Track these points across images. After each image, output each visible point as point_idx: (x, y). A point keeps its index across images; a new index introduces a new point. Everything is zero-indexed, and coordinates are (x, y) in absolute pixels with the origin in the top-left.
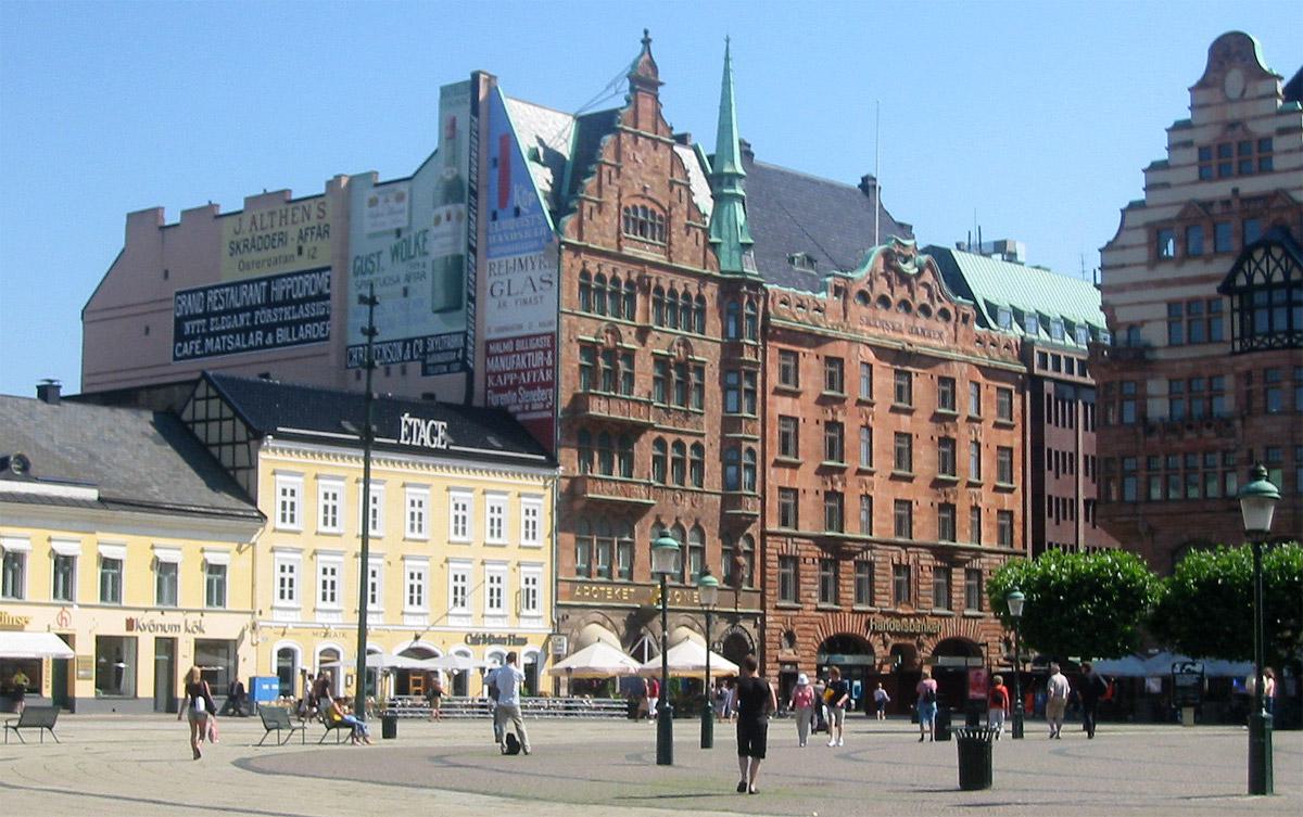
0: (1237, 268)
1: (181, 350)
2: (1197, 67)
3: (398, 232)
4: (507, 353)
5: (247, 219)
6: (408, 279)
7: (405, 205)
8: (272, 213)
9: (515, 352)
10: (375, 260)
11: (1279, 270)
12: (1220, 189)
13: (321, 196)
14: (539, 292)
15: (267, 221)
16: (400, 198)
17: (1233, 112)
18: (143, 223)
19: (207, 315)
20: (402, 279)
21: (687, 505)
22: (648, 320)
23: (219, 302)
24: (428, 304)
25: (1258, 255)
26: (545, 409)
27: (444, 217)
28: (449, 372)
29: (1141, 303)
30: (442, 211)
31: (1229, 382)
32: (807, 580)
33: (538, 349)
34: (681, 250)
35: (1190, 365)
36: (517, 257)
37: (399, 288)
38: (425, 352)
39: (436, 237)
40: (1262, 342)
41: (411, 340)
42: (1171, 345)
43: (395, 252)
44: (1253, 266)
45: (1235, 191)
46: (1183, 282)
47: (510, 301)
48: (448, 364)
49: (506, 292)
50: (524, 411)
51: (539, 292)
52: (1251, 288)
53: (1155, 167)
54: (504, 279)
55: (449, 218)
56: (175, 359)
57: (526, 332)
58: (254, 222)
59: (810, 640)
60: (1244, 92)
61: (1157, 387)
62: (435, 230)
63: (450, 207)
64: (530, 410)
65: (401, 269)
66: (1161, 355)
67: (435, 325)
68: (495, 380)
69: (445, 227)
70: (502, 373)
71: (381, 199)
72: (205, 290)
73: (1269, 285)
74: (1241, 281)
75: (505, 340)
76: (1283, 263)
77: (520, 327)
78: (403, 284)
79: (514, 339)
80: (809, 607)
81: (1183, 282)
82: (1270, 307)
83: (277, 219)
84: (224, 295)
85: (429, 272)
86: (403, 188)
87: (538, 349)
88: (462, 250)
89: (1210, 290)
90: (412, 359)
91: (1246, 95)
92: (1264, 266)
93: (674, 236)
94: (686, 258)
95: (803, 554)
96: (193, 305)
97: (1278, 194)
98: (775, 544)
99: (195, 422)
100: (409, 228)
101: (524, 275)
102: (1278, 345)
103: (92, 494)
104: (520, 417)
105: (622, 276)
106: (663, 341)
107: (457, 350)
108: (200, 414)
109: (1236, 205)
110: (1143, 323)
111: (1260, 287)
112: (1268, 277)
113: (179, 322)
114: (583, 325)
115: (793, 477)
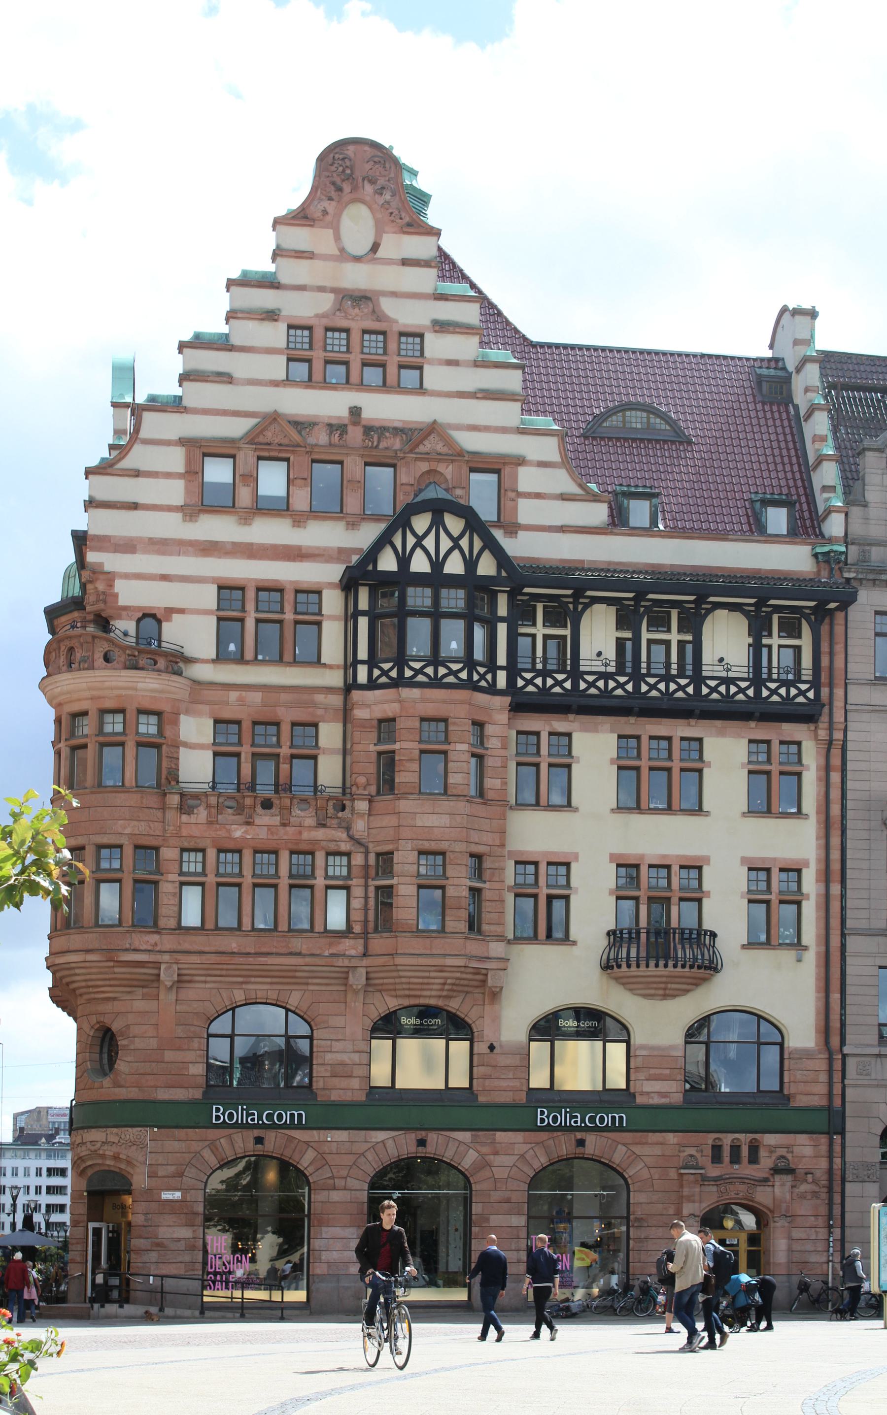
0: (384, 540)
2: (296, 186)
11: (456, 554)
12: (330, 404)
17: (356, 277)
25: (421, 523)
29: (165, 578)
31: (330, 734)
35: (256, 697)
40: (420, 671)
42: (221, 657)
44: (411, 541)
45: (355, 412)
46: (251, 551)
52: (405, 576)
53: (198, 343)
60: (375, 247)
61: (195, 729)
66: (204, 672)
73: (436, 579)
74: (388, 562)
76: (464, 543)
81: (251, 551)
82: (436, 615)
89: (334, 572)
91: (381, 253)
92: (429, 543)
97: (433, 429)
102: (451, 679)
109: (355, 435)
110: (170, 611)
111: (420, 580)
112: (437, 564)
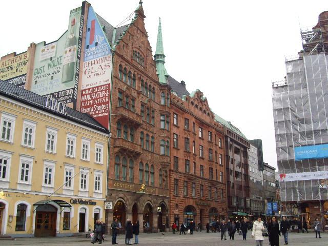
4: (90, 94)
9: (93, 92)
10: (42, 69)
20: (51, 73)
26: (105, 112)
33: (103, 90)
36: (96, 59)
37: (50, 76)
38: (58, 97)
41: (53, 94)
43: (49, 65)
48: (66, 100)
49: (91, 72)
50: (96, 114)
54: (90, 68)
55: (70, 51)
64: (99, 114)
65: (51, 70)
68: (84, 104)
69: (69, 53)
71: (46, 49)
75: (90, 89)
79: (93, 88)
85: (61, 70)
87: (103, 90)
104: (95, 116)
105: (132, 72)
107: (70, 95)
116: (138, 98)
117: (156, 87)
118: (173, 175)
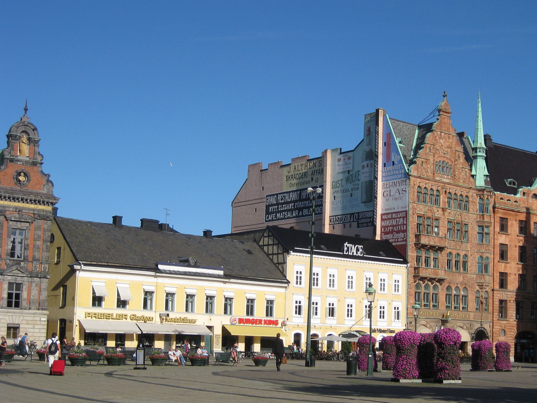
1: (268, 218)
3: (349, 171)
5: (292, 167)
6: (352, 190)
7: (351, 161)
8: (301, 165)
9: (392, 218)
13: (320, 158)
14: (401, 195)
15: (300, 168)
16: (349, 158)
18: (258, 171)
19: (278, 204)
20: (350, 190)
21: (461, 279)
22: (445, 205)
23: (282, 199)
24: (360, 199)
27: (366, 166)
28: (367, 226)
30: (365, 163)
32: (511, 309)
34: (459, 178)
36: (393, 181)
37: (349, 193)
38: (358, 218)
39: (363, 173)
41: (353, 214)
47: (391, 198)
48: (367, 223)
49: (389, 195)
50: (395, 242)
51: (401, 195)
54: (388, 190)
55: (367, 166)
56: (266, 221)
57: (396, 210)
58: (295, 168)
59: (512, 333)
62: (362, 171)
63: (368, 162)
64: (398, 241)
67: (362, 208)
68: (384, 230)
69: (366, 169)
70: (387, 227)
72: (277, 195)
75: (389, 214)
77: (394, 209)
78: (351, 192)
79: (392, 213)
80: (511, 320)
83: (303, 167)
84: (284, 197)
85: (360, 187)
86: (350, 154)
87: (401, 217)
88: (373, 179)
90: (354, 221)
93: (456, 173)
94: (461, 181)
95: (510, 299)
96: (273, 200)
98: (497, 295)
99: (264, 245)
100: (353, 170)
101: (396, 188)
103: (221, 273)
104: (394, 244)
105: (435, 188)
106: (453, 214)
107: (370, 218)
108: (266, 243)
113: (268, 207)
114: (419, 208)
115: (505, 267)
116: (444, 215)
117: (470, 195)
118: (499, 295)
